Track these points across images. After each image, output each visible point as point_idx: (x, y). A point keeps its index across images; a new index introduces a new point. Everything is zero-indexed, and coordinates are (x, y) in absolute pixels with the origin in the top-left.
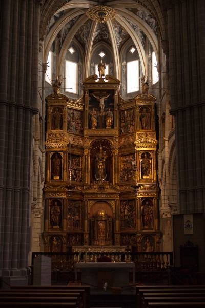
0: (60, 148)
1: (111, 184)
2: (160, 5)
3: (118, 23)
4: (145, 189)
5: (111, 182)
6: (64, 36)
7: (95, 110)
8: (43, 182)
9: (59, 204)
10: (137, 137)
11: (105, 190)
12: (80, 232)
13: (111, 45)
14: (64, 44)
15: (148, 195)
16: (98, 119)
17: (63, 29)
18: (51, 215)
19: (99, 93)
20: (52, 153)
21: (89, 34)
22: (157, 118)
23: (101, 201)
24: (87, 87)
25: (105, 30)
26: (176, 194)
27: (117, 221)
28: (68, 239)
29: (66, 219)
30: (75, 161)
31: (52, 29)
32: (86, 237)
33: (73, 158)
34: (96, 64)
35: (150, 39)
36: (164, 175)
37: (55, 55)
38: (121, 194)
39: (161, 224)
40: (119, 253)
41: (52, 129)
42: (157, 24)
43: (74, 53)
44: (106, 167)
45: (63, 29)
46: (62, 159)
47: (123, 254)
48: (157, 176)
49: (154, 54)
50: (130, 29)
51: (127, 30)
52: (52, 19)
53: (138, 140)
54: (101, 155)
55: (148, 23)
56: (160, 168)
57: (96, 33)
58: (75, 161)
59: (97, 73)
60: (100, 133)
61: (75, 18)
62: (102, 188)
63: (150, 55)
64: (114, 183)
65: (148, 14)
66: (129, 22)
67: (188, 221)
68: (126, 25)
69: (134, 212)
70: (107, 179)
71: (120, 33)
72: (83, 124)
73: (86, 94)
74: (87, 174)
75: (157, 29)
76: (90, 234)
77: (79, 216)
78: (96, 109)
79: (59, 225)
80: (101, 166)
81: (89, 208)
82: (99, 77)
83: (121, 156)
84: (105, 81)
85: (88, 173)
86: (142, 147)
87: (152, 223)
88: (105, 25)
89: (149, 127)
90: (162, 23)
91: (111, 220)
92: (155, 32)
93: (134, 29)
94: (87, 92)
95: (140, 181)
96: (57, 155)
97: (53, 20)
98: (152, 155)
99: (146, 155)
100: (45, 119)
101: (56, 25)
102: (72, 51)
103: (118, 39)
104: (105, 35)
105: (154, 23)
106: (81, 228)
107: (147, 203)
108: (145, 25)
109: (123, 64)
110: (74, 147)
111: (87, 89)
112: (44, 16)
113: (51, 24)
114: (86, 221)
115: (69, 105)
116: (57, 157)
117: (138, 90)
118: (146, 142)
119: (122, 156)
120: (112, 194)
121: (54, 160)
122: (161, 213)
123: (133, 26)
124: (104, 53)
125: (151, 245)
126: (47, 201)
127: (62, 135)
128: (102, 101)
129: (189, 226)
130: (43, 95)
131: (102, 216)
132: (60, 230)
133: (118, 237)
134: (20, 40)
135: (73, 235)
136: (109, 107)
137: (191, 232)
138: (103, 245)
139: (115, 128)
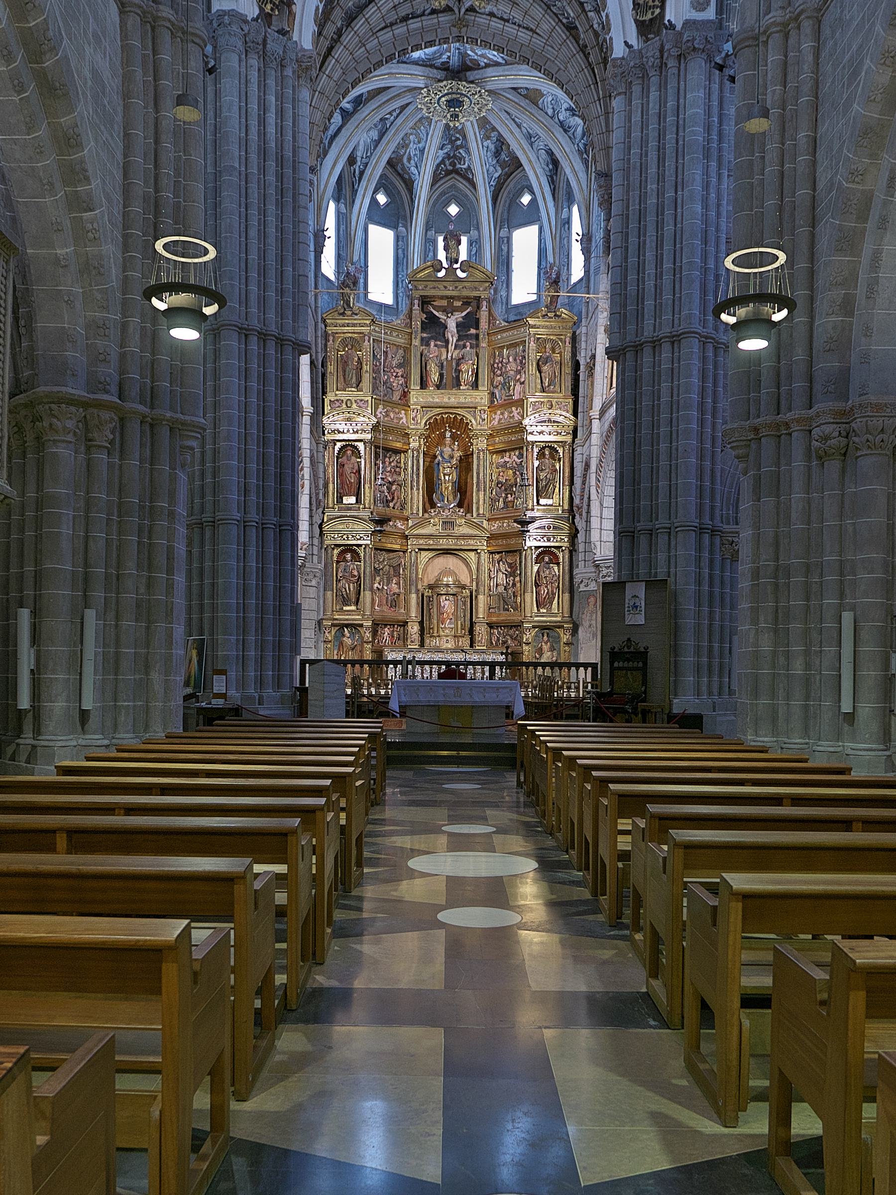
0: (357, 432)
1: (469, 515)
3: (494, 129)
4: (543, 528)
5: (469, 510)
7: (436, 345)
8: (321, 510)
9: (356, 557)
10: (530, 410)
11: (456, 528)
12: (401, 618)
13: (474, 185)
14: (364, 183)
15: (549, 540)
16: (442, 366)
17: (362, 143)
18: (338, 581)
19: (444, 303)
20: (339, 445)
22: (576, 366)
23: (447, 552)
24: (416, 289)
25: (461, 146)
26: (612, 538)
27: (481, 597)
28: (375, 633)
29: (371, 589)
30: (390, 463)
32: (414, 629)
33: (385, 457)
34: (438, 232)
35: (568, 171)
36: (586, 497)
38: (492, 537)
39: (576, 604)
40: (483, 664)
41: (337, 390)
43: (387, 205)
44: (459, 477)
45: (362, 143)
46: (360, 458)
47: (492, 665)
48: (571, 499)
49: (575, 209)
51: (514, 146)
52: (336, 114)
53: (532, 417)
54: (447, 450)
56: (578, 481)
57: (441, 153)
58: (390, 463)
59: (442, 255)
60: (446, 400)
61: (390, 113)
62: (448, 524)
64: (475, 515)
65: (565, 106)
67: (635, 596)
68: (512, 133)
69: (517, 579)
70: (460, 505)
71: (497, 153)
72: (407, 377)
74: (416, 493)
75: (585, 145)
76: (421, 623)
77: (398, 584)
78: (439, 343)
79: (357, 604)
80: (447, 477)
81: (421, 567)
82: (445, 265)
83: (492, 453)
85: (418, 489)
86: (540, 433)
87: (555, 601)
89: (557, 388)
91: (467, 592)
93: (531, 144)
94: (416, 302)
95: (533, 510)
96: (349, 447)
97: (337, 119)
98: (561, 451)
99: (548, 451)
100: (322, 366)
102: (382, 199)
103: (492, 169)
104: (461, 159)
105: (580, 130)
106: (402, 611)
107: (547, 559)
108: (559, 133)
109: (504, 233)
110: (389, 430)
111: (417, 294)
114: (414, 596)
115: (376, 331)
116: (349, 452)
117: (534, 297)
118: (550, 421)
119: (494, 453)
120: (471, 537)
121: (343, 460)
122: (577, 580)
123: (530, 138)
124: (459, 204)
125: (552, 649)
126: (329, 551)
127: (361, 404)
128: (452, 324)
129: (635, 607)
130: (316, 307)
131: (447, 585)
132: (358, 615)
133: (481, 630)
134: (263, 170)
135: (386, 625)
136: (469, 337)
137: (640, 619)
138: (449, 646)
139: (480, 388)
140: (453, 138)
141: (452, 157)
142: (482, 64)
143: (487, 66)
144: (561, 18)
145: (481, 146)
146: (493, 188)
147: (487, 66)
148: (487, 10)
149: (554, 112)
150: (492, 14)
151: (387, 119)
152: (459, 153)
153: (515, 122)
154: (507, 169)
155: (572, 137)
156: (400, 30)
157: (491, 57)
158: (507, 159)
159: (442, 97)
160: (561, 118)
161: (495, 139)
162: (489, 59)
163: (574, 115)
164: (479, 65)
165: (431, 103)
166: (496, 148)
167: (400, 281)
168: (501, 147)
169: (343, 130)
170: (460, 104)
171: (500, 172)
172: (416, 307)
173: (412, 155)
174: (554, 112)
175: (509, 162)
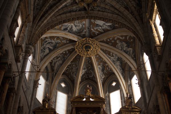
2: (137, 21)
6: (57, 70)
14: (56, 76)
21: (78, 70)
25: (90, 69)
31: (45, 58)
37: (48, 83)
42: (134, 51)
43: (65, 87)
50: (111, 63)
55: (126, 52)
63: (129, 81)
66: (110, 58)
68: (108, 60)
71: (103, 70)
73: (74, 111)
84: (91, 99)
88: (90, 58)
90: (141, 33)
92: (133, 58)
93: (115, 64)
94: (74, 109)
97: (47, 51)
101: (50, 55)
102: (63, 85)
103: (101, 75)
104: (91, 74)
105: (131, 51)
108: (124, 54)
109: (106, 95)
112: (37, 30)
113: (45, 53)
140: (88, 66)
141: (88, 73)
142: (96, 34)
143: (98, 34)
144: (122, 5)
145: (97, 68)
146: (102, 81)
147: (98, 34)
148: (97, 10)
149: (122, 48)
150: (99, 11)
151: (65, 57)
152: (90, 71)
153: (109, 57)
154: (106, 76)
155: (129, 54)
156: (68, 15)
157: (99, 30)
158: (106, 72)
159: (84, 45)
160: (124, 49)
161: (102, 65)
162: (99, 31)
163: (129, 47)
164: (95, 34)
165: (80, 48)
166: (102, 69)
167: (69, 110)
168: (104, 68)
169: (49, 54)
170: (90, 48)
171: (104, 77)
172: (74, 111)
173: (74, 72)
174: (122, 48)
175: (107, 73)
